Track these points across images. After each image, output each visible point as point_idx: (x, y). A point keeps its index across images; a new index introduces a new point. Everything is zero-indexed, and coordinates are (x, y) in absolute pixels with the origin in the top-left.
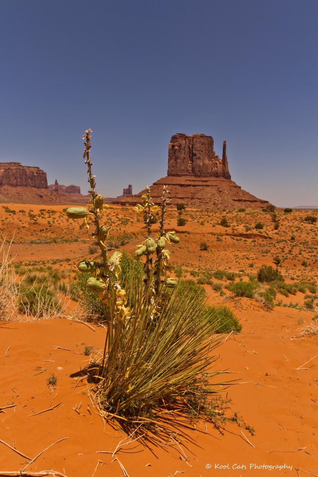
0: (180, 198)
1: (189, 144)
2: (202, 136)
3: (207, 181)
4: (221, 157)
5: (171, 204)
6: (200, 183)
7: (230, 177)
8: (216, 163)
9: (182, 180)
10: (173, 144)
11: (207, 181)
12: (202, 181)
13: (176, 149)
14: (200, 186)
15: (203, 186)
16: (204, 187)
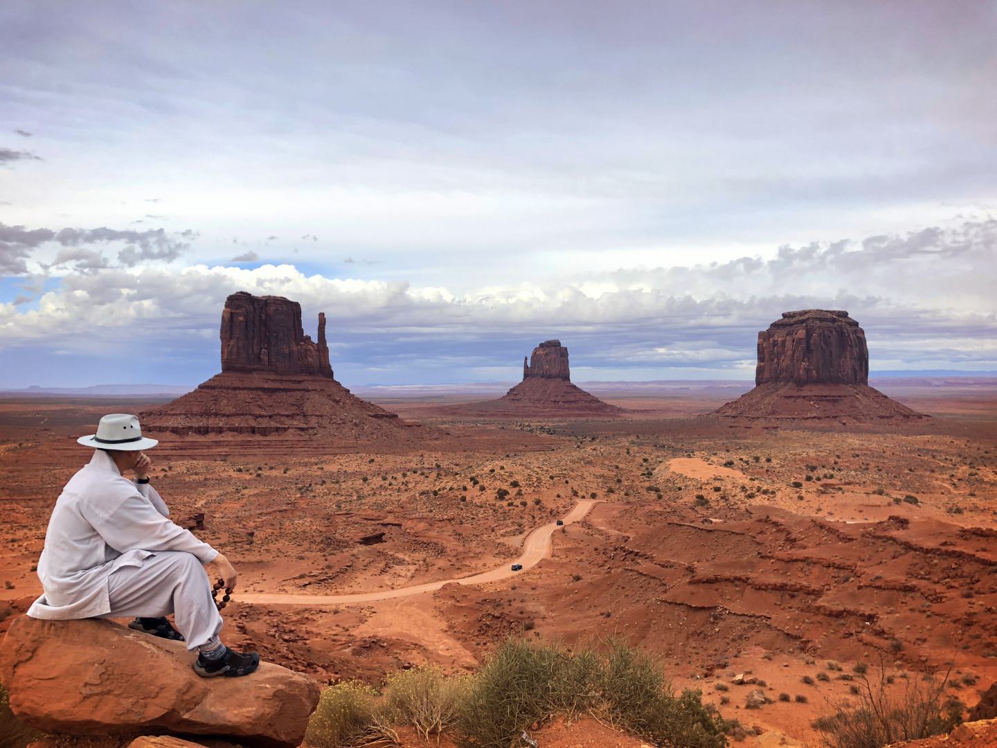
0: (287, 416)
1: (261, 312)
2: (284, 301)
3: (300, 382)
4: (315, 340)
5: (289, 428)
6: (291, 386)
7: (332, 373)
8: (310, 350)
9: (257, 380)
10: (233, 311)
11: (300, 382)
12: (294, 382)
13: (241, 321)
14: (294, 390)
15: (299, 390)
16: (302, 392)
